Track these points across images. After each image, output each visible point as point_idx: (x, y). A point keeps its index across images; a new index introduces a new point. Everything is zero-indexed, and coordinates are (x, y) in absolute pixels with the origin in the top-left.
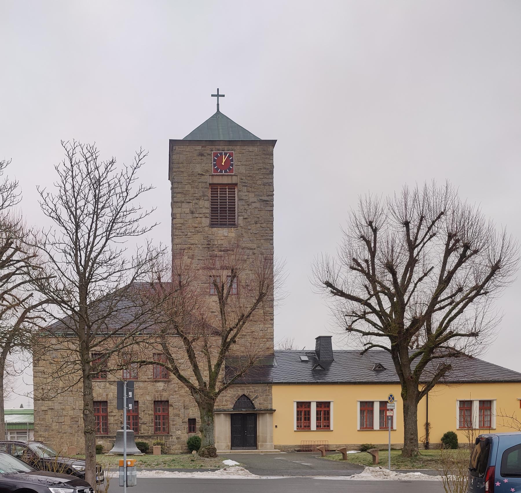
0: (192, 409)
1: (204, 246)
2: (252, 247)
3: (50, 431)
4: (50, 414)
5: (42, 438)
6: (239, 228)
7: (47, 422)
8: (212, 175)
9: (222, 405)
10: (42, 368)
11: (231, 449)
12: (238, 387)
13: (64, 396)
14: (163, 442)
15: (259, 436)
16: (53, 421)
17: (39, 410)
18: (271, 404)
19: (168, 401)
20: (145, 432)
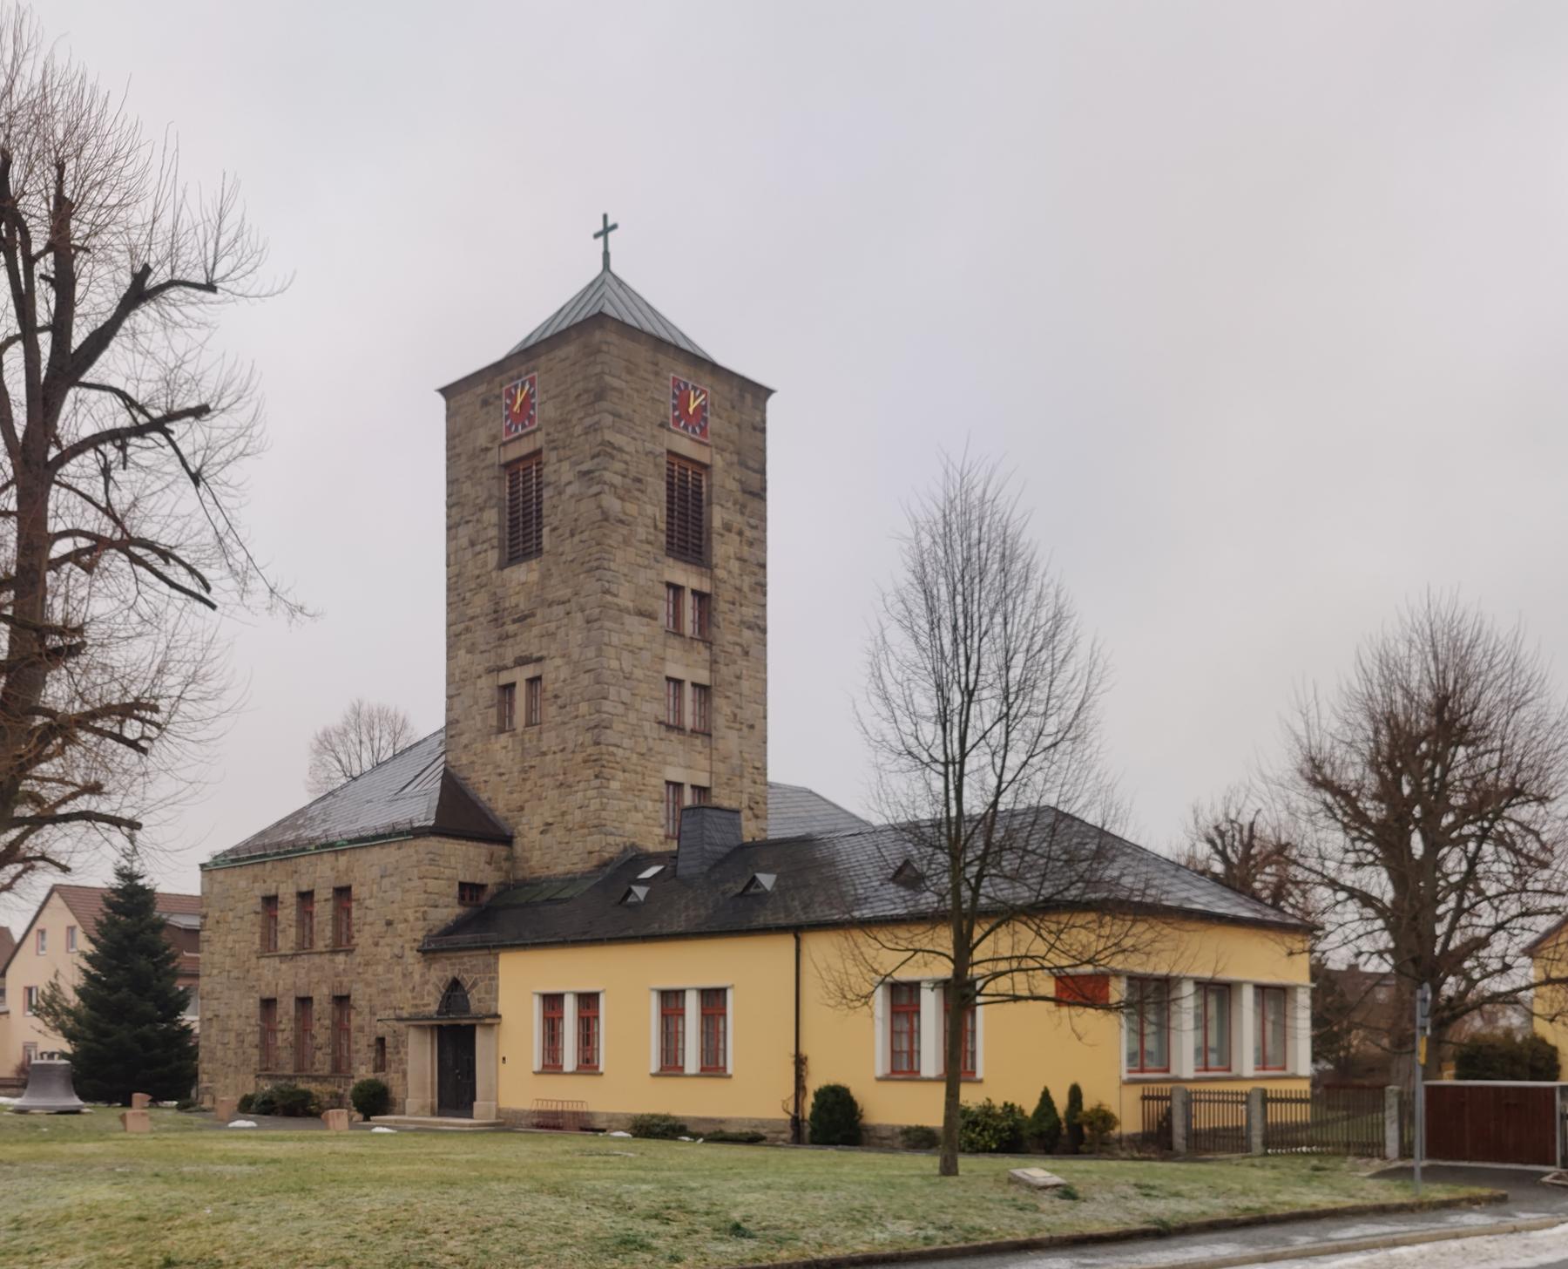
1: (489, 618)
2: (566, 598)
6: (544, 556)
8: (504, 444)
9: (425, 1005)
11: (440, 1115)
12: (448, 959)
14: (341, 1091)
18: (496, 1000)
19: (348, 997)
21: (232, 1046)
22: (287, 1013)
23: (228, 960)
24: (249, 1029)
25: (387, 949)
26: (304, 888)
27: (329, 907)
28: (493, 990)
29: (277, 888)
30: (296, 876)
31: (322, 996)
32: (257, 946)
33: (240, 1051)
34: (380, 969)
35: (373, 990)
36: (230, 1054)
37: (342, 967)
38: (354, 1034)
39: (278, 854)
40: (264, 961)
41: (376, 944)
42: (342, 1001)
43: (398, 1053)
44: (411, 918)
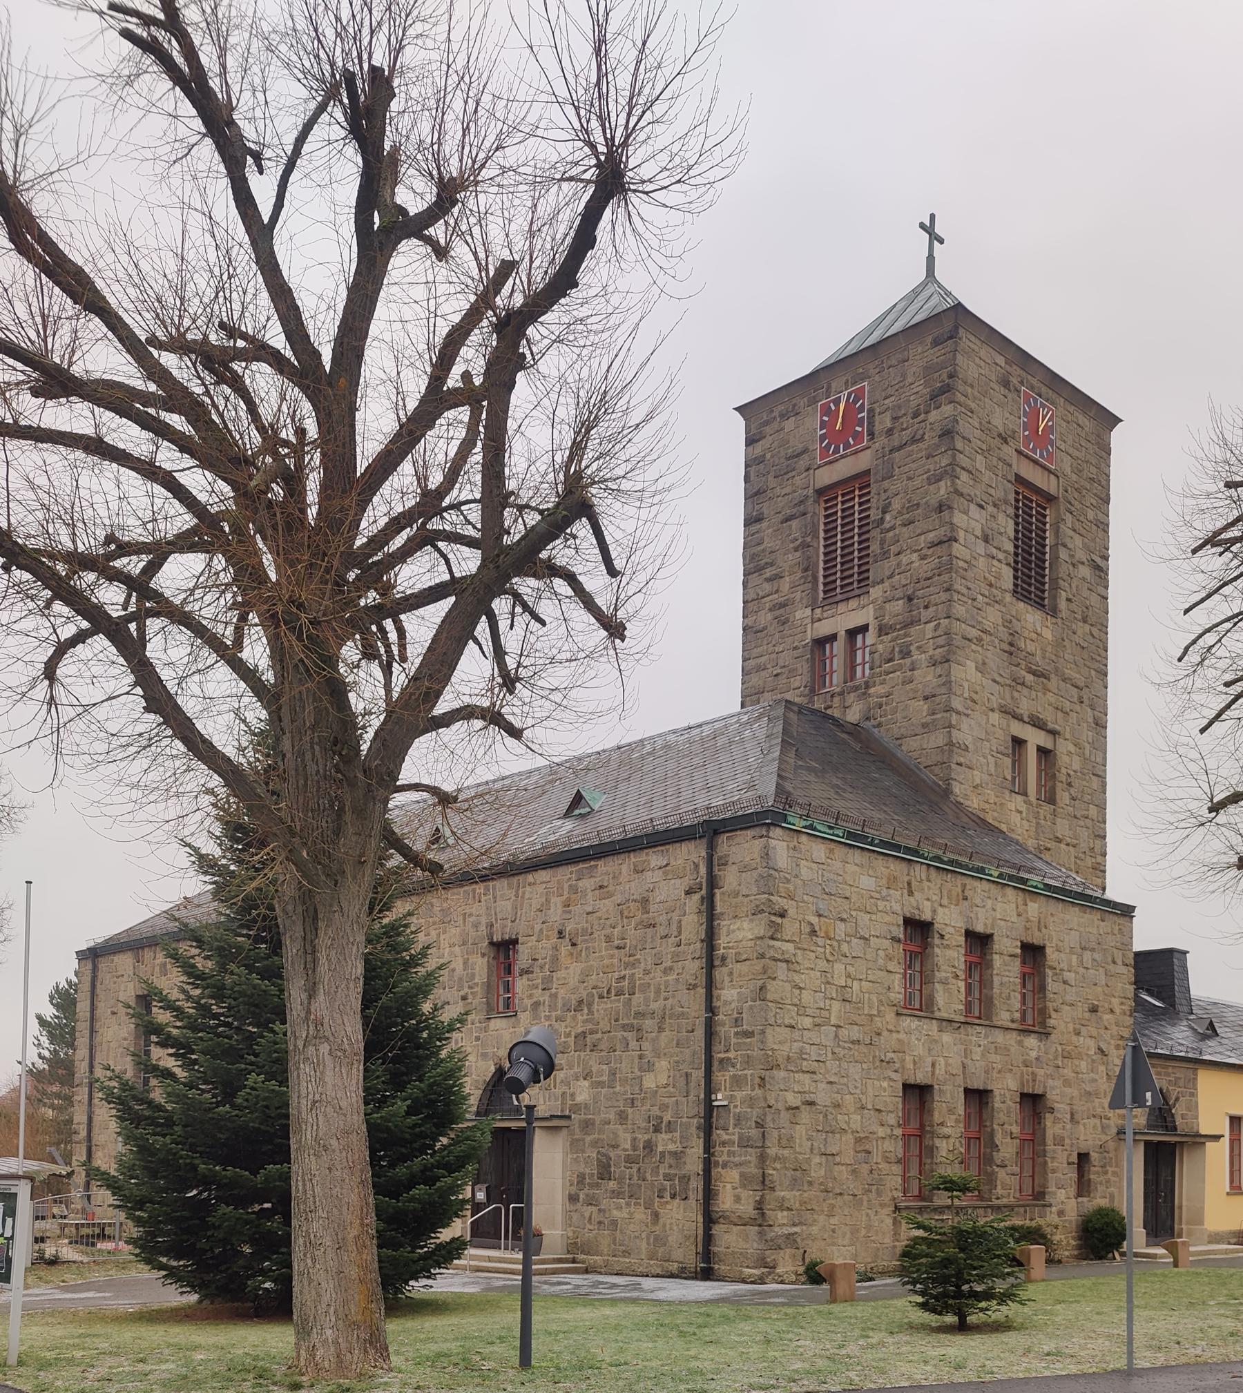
0: (1084, 1125)
3: (805, 1188)
4: (804, 1121)
5: (785, 1213)
7: (798, 1150)
10: (789, 947)
13: (839, 1059)
15: (1180, 1207)
16: (812, 1149)
17: (780, 1106)
20: (1005, 1192)
21: (848, 1156)
22: (951, 1111)
23: (836, 1006)
24: (881, 1132)
25: (1091, 1043)
26: (980, 928)
27: (1016, 967)
28: (1193, 1107)
29: (934, 911)
30: (966, 903)
31: (1005, 1090)
32: (897, 995)
33: (865, 1169)
34: (1083, 1065)
35: (1072, 1091)
36: (842, 1173)
37: (1034, 1054)
38: (1050, 1147)
39: (937, 858)
40: (908, 1023)
41: (1078, 1034)
42: (1033, 1103)
43: (1106, 1173)
44: (1117, 1011)
